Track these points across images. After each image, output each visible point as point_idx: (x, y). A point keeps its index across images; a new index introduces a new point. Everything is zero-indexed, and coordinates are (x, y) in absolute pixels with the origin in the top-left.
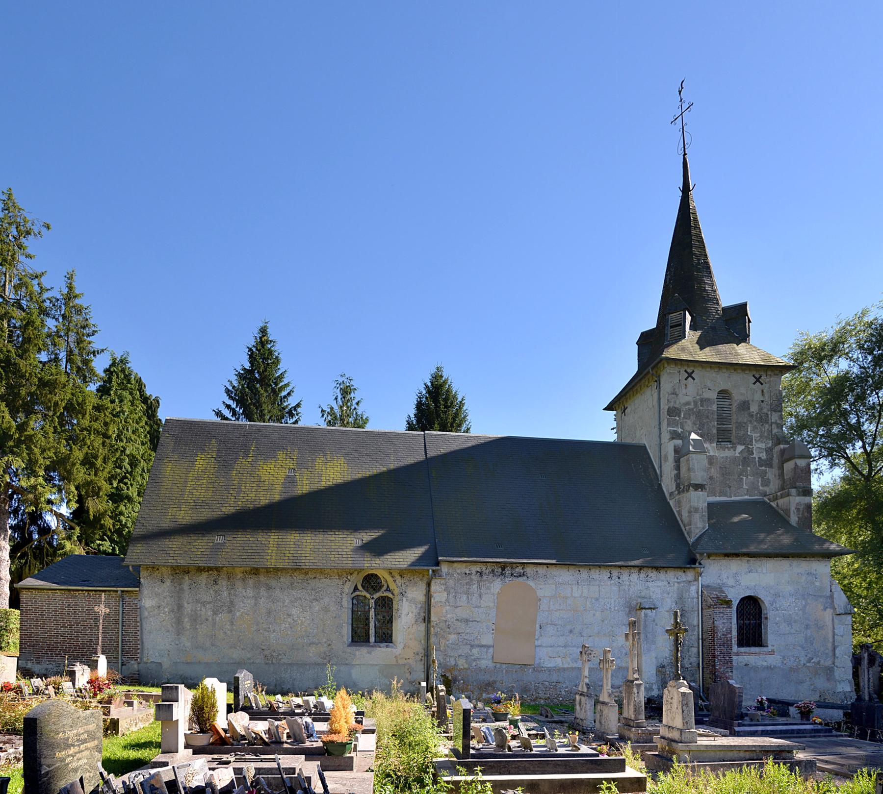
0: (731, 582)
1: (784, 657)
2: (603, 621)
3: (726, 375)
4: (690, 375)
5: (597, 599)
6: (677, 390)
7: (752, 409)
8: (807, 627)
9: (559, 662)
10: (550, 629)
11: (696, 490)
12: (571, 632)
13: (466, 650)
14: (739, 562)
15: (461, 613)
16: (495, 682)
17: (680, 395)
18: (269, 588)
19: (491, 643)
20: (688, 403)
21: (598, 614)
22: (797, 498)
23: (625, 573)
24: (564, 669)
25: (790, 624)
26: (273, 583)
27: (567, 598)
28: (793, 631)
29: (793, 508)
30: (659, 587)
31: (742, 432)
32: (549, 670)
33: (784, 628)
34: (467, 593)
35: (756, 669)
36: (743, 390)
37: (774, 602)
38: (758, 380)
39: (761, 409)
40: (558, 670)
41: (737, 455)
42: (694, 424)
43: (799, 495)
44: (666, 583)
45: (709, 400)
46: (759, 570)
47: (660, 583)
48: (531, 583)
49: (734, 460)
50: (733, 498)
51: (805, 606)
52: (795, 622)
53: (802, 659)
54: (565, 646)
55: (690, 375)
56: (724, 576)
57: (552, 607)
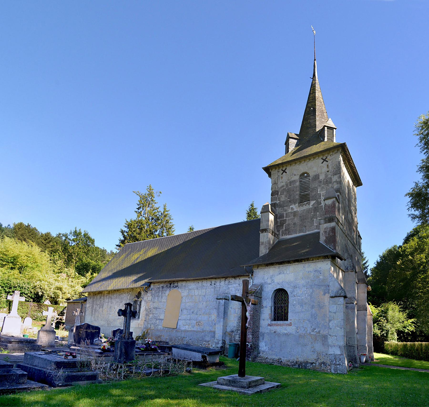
0: (269, 281)
1: (297, 328)
2: (206, 307)
3: (305, 164)
4: (284, 171)
5: (204, 296)
6: (277, 182)
7: (321, 178)
8: (313, 307)
9: (187, 328)
10: (185, 311)
11: (262, 232)
12: (193, 312)
13: (154, 321)
14: (274, 268)
15: (156, 305)
16: (161, 336)
17: (279, 183)
18: (111, 299)
19: (163, 318)
20: (283, 186)
21: (204, 303)
22: (325, 225)
23: (218, 281)
24: (188, 331)
25: (302, 306)
26: (112, 297)
27: (192, 296)
28: (303, 310)
29: (322, 232)
30: (234, 287)
31: (314, 193)
32: (182, 331)
33: (298, 308)
34: (158, 296)
35: (279, 335)
36: (315, 169)
37: (293, 291)
38: (324, 160)
39: (326, 176)
40: (186, 331)
41: (311, 207)
42: (286, 196)
43: (326, 223)
44: (237, 285)
45: (294, 181)
46: (285, 272)
47: (235, 285)
48: (180, 290)
49: (309, 211)
50: (308, 233)
51: (312, 293)
52: (305, 304)
53: (309, 329)
54: (190, 320)
55: (284, 171)
56: (266, 278)
57: (186, 301)
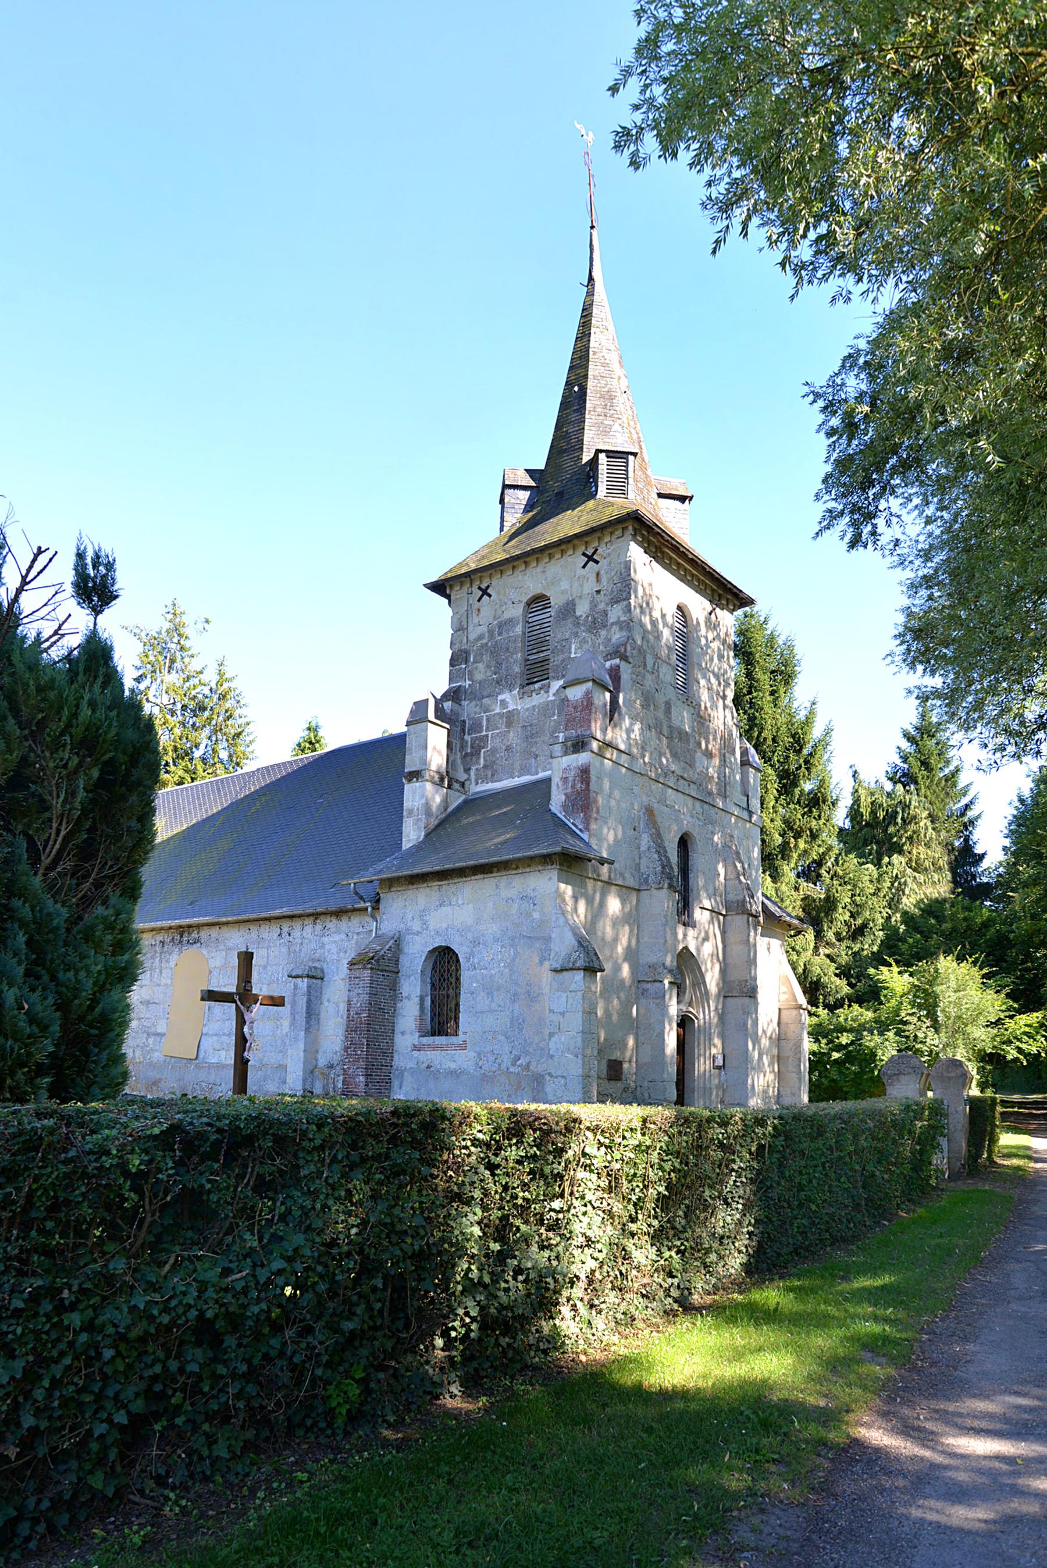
0: (416, 926)
1: (479, 1054)
3: (539, 569)
4: (485, 592)
6: (464, 623)
8: (515, 997)
11: (410, 781)
14: (428, 890)
16: (160, 1080)
17: (470, 628)
20: (481, 637)
25: (490, 994)
28: (494, 1006)
29: (556, 780)
33: (482, 1001)
36: (564, 585)
37: (472, 954)
38: (590, 558)
39: (594, 605)
41: (551, 698)
42: (488, 667)
43: (566, 754)
44: (343, 936)
45: (511, 620)
47: (337, 937)
51: (514, 960)
52: (498, 989)
53: (505, 1058)
55: (485, 592)
56: (409, 917)
